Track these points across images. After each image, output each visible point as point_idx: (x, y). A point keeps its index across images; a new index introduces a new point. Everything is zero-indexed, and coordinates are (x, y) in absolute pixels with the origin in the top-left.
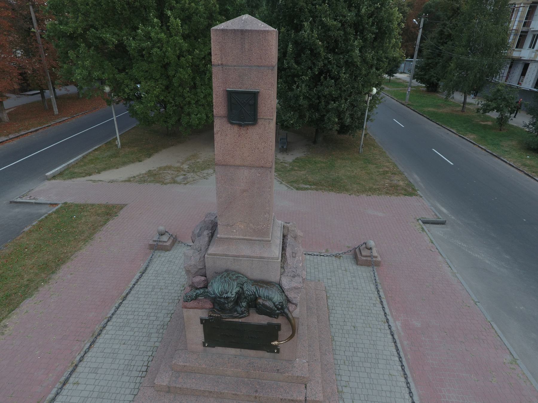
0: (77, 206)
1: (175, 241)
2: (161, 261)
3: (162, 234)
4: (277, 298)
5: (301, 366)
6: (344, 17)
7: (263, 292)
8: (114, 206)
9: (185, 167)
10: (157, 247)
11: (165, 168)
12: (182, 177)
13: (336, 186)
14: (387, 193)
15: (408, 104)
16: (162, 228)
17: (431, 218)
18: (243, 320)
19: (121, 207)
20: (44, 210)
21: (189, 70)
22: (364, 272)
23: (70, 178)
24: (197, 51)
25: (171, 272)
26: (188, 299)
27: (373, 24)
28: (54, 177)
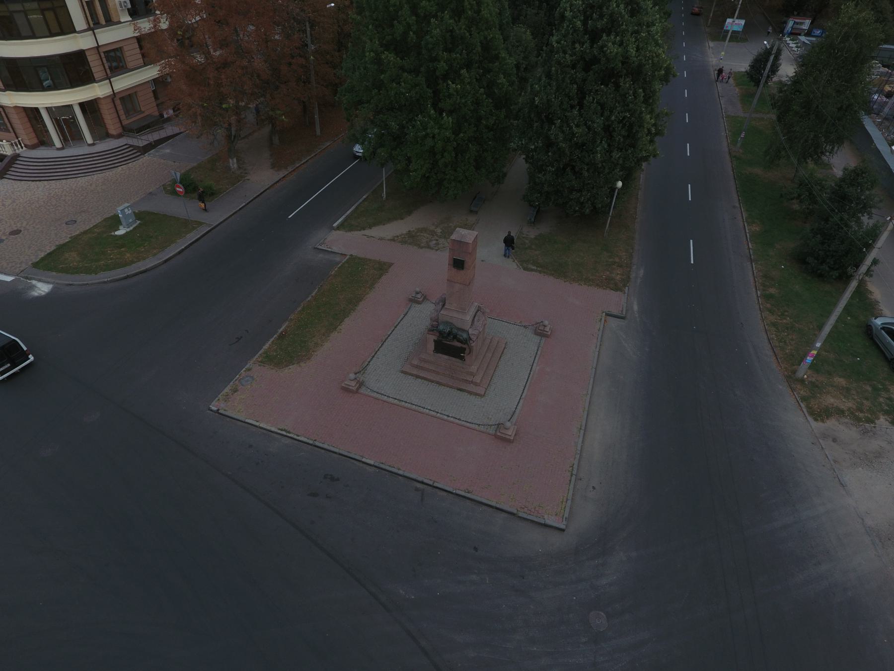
0: (359, 258)
1: (425, 298)
2: (416, 309)
3: (417, 293)
4: (465, 336)
5: (474, 368)
6: (593, 122)
7: (460, 333)
8: (385, 263)
9: (439, 231)
10: (413, 301)
11: (424, 230)
12: (434, 242)
13: (559, 271)
14: (597, 285)
15: (735, 157)
16: (418, 289)
17: (615, 312)
18: (450, 344)
19: (390, 265)
20: (338, 259)
21: (453, 154)
22: (537, 339)
23: (350, 230)
24: (462, 135)
25: (421, 317)
26: (430, 330)
27: (623, 127)
28: (338, 228)
